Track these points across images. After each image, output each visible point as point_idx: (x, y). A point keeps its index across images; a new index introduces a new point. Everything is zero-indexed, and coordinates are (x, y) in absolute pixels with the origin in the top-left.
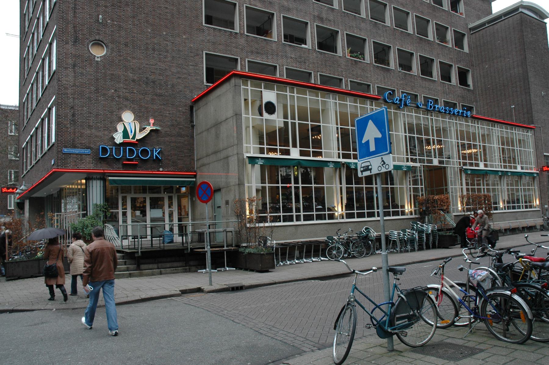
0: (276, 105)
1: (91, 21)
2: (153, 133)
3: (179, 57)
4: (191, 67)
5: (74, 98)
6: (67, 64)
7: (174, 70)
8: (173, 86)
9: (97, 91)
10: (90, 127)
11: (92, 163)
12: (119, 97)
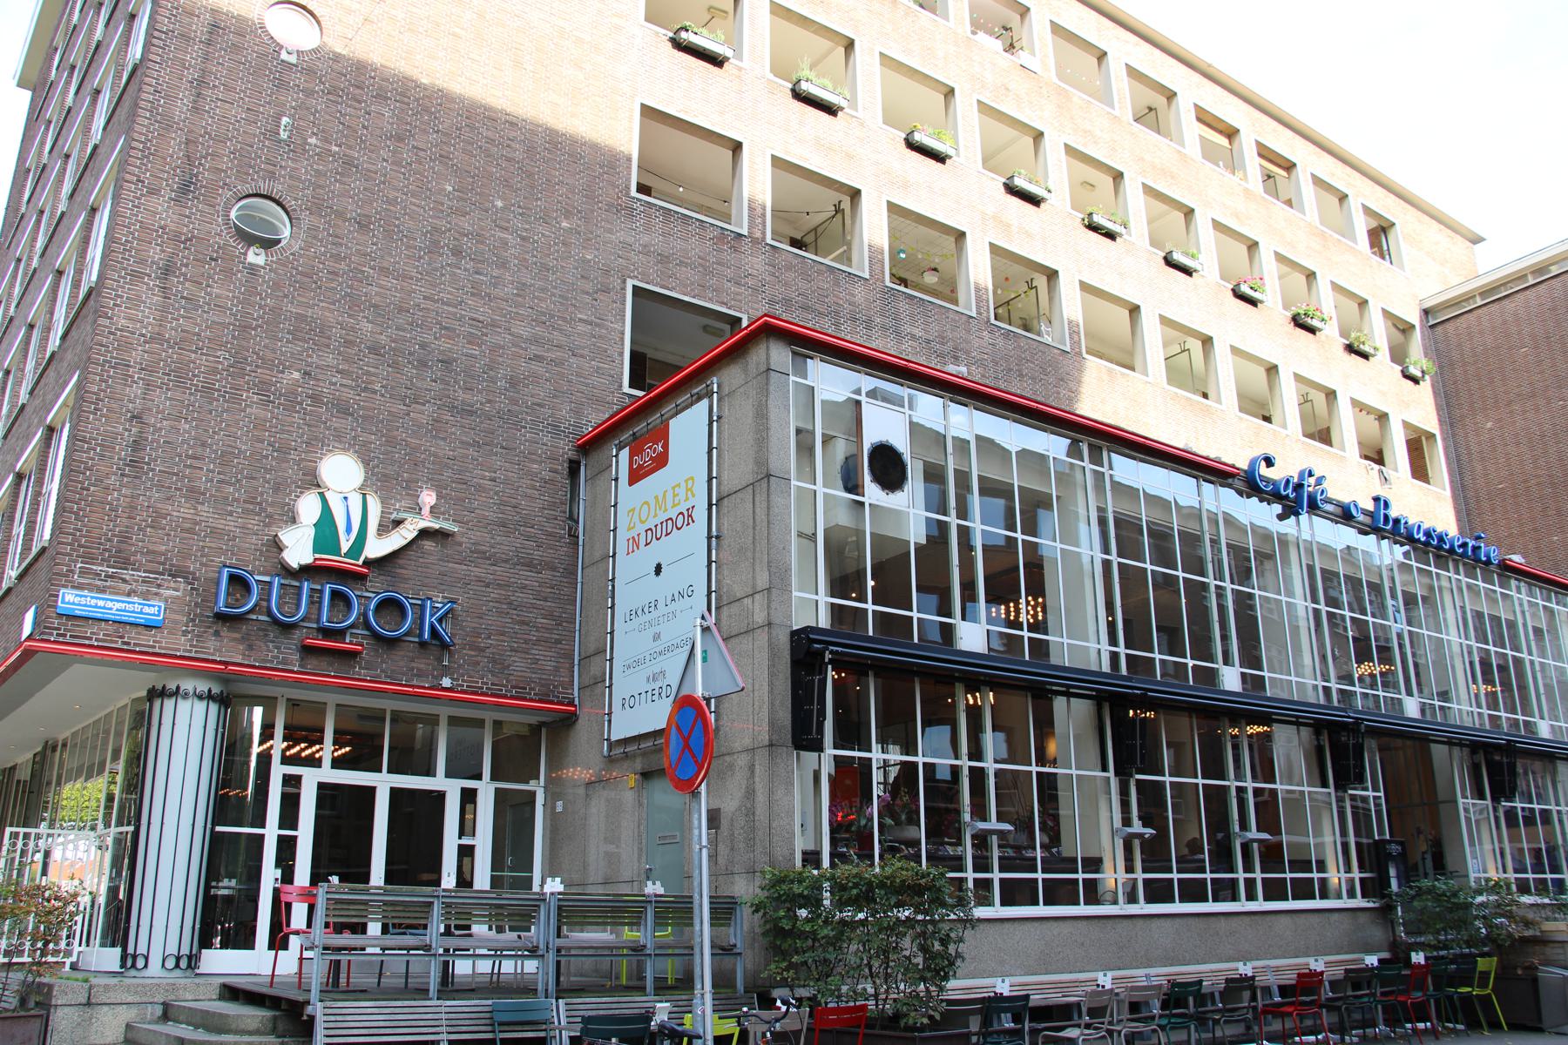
0: (907, 457)
1: (252, 129)
2: (428, 545)
3: (543, 290)
4: (581, 327)
5: (148, 385)
6: (142, 262)
7: (523, 330)
8: (513, 383)
9: (238, 365)
10: (194, 495)
11: (185, 633)
12: (316, 399)
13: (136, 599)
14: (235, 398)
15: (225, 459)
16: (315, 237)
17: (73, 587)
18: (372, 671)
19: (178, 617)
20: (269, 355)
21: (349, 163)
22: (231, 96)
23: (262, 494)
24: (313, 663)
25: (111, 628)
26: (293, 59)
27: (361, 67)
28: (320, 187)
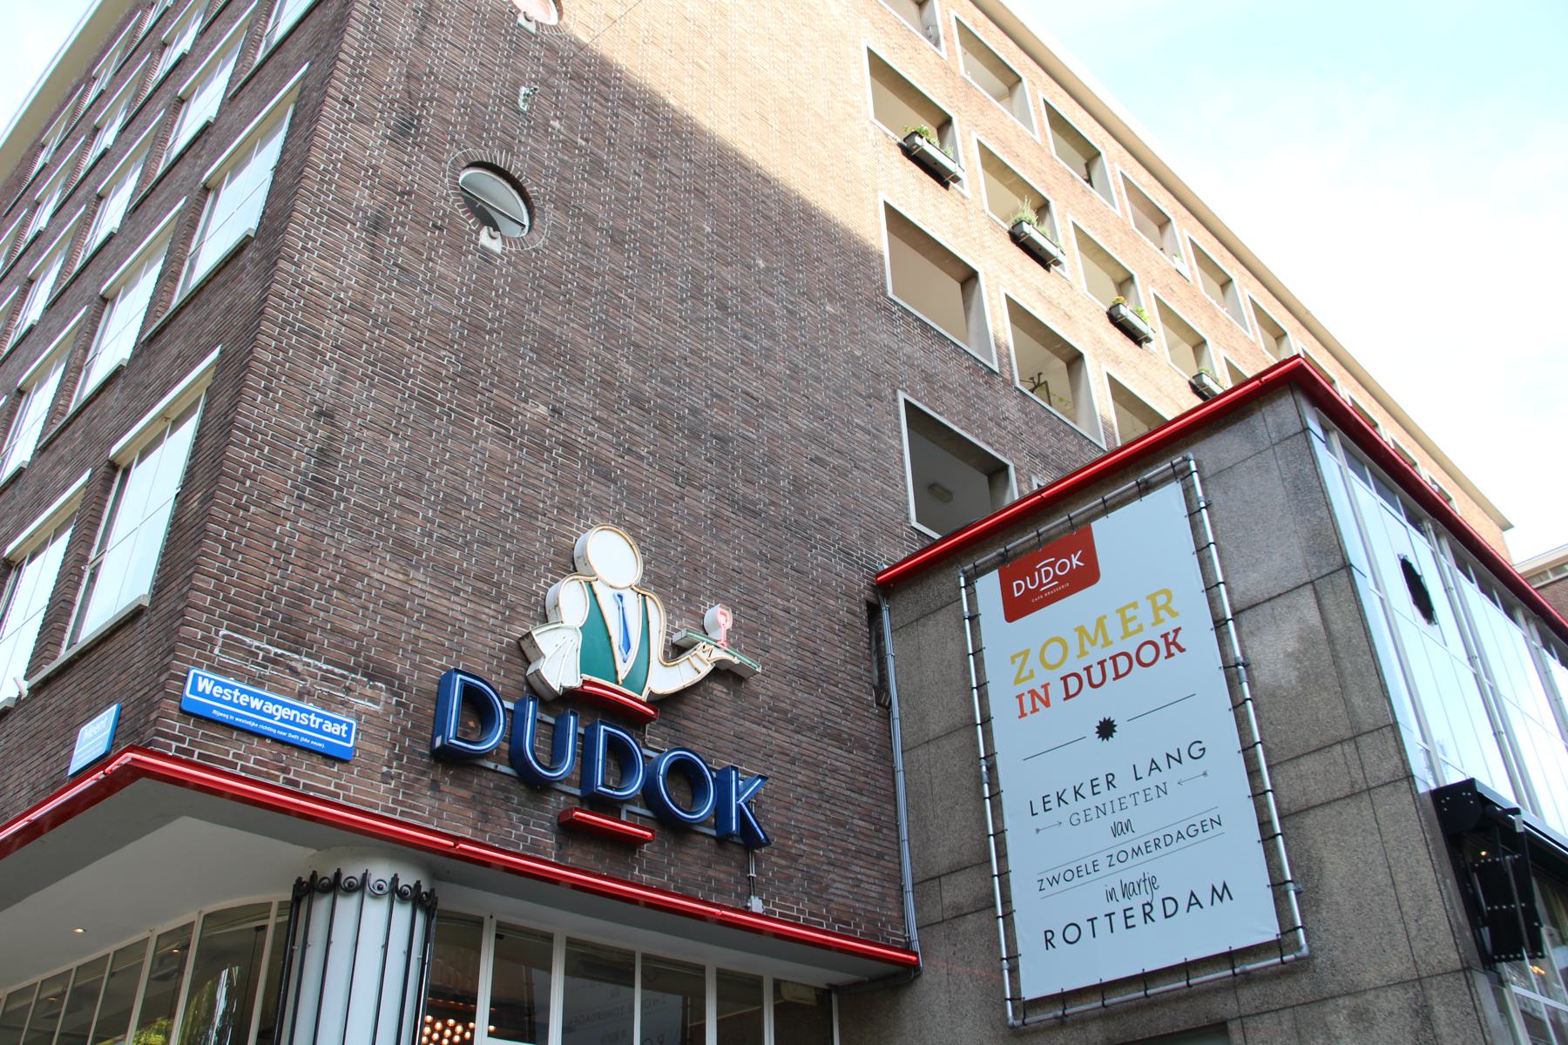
1: (486, 87)
2: (718, 689)
4: (860, 435)
6: (346, 203)
7: (803, 424)
8: (798, 486)
9: (467, 380)
10: (404, 551)
11: (386, 778)
12: (569, 447)
13: (310, 707)
14: (462, 421)
15: (450, 505)
16: (562, 239)
17: (211, 669)
18: (660, 873)
19: (375, 748)
20: (508, 373)
21: (597, 163)
22: (461, 42)
23: (500, 570)
24: (575, 855)
25: (268, 751)
26: (532, 27)
27: (604, 65)
28: (565, 179)
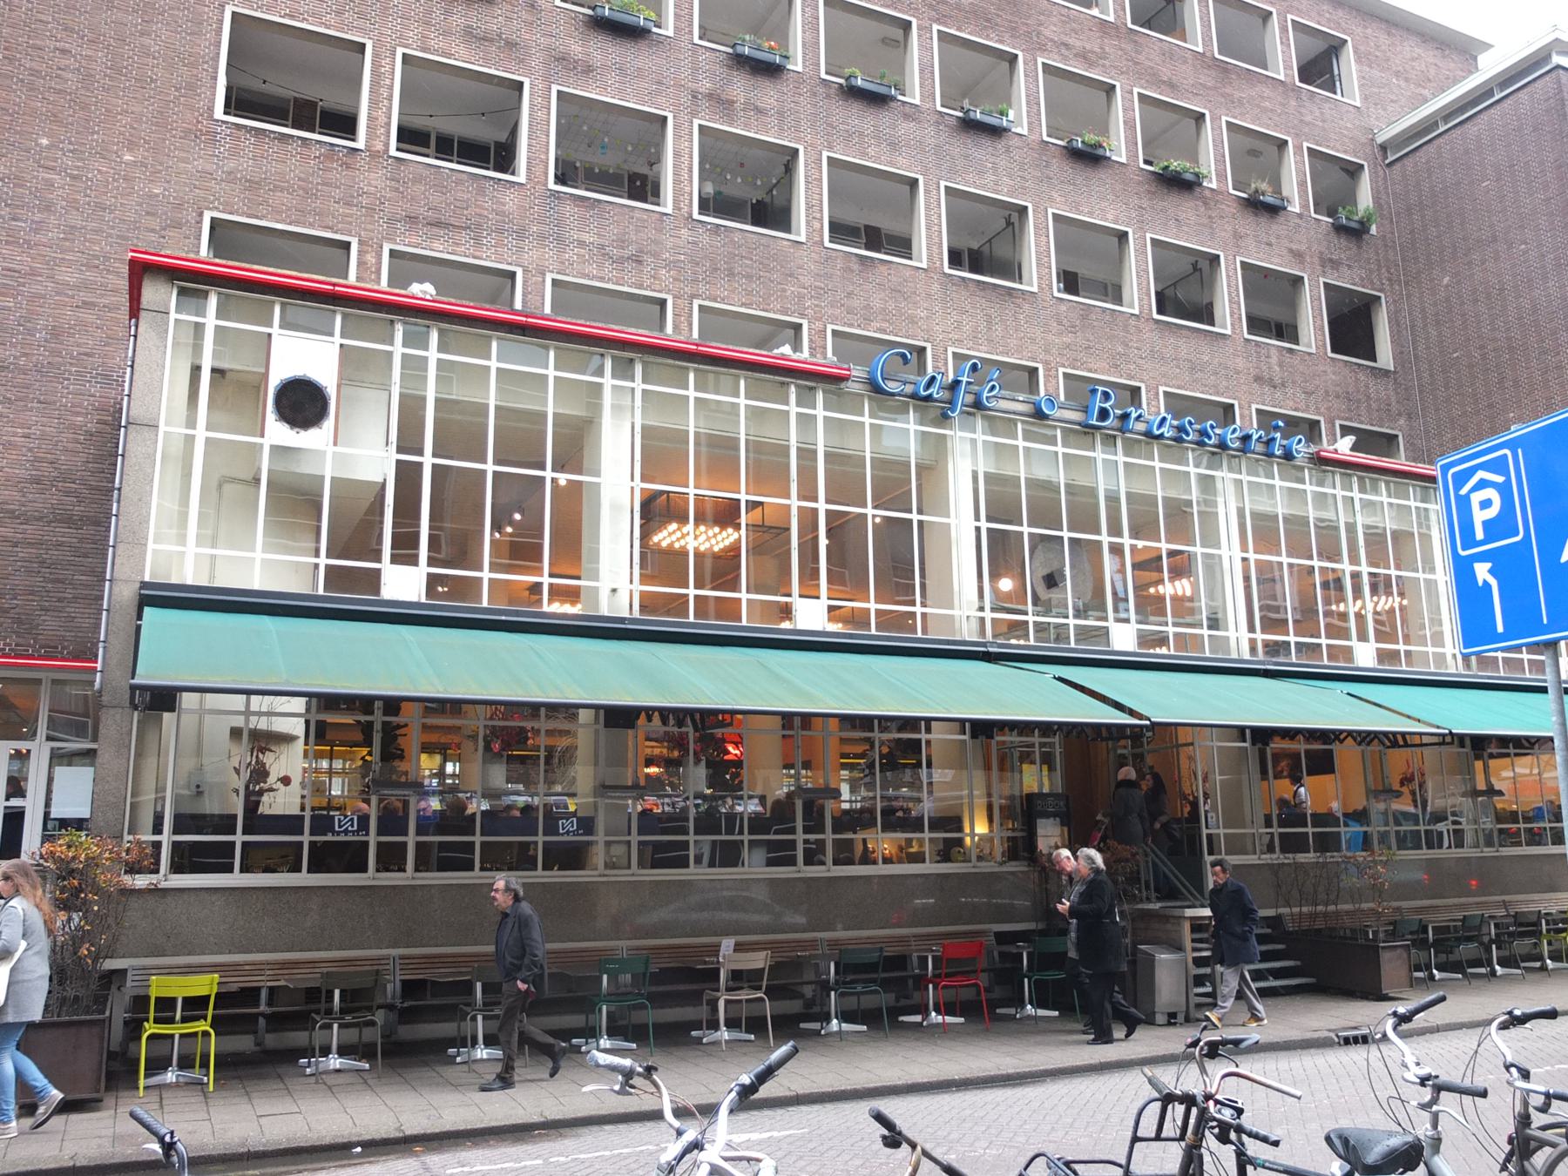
0: (332, 392)
3: (96, 231)
7: (69, 276)
8: (55, 333)
